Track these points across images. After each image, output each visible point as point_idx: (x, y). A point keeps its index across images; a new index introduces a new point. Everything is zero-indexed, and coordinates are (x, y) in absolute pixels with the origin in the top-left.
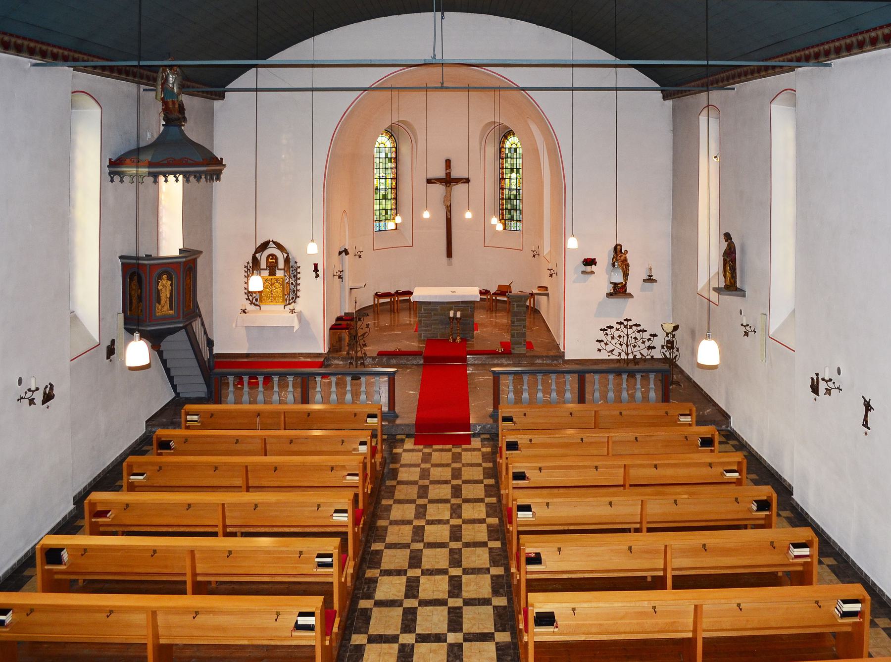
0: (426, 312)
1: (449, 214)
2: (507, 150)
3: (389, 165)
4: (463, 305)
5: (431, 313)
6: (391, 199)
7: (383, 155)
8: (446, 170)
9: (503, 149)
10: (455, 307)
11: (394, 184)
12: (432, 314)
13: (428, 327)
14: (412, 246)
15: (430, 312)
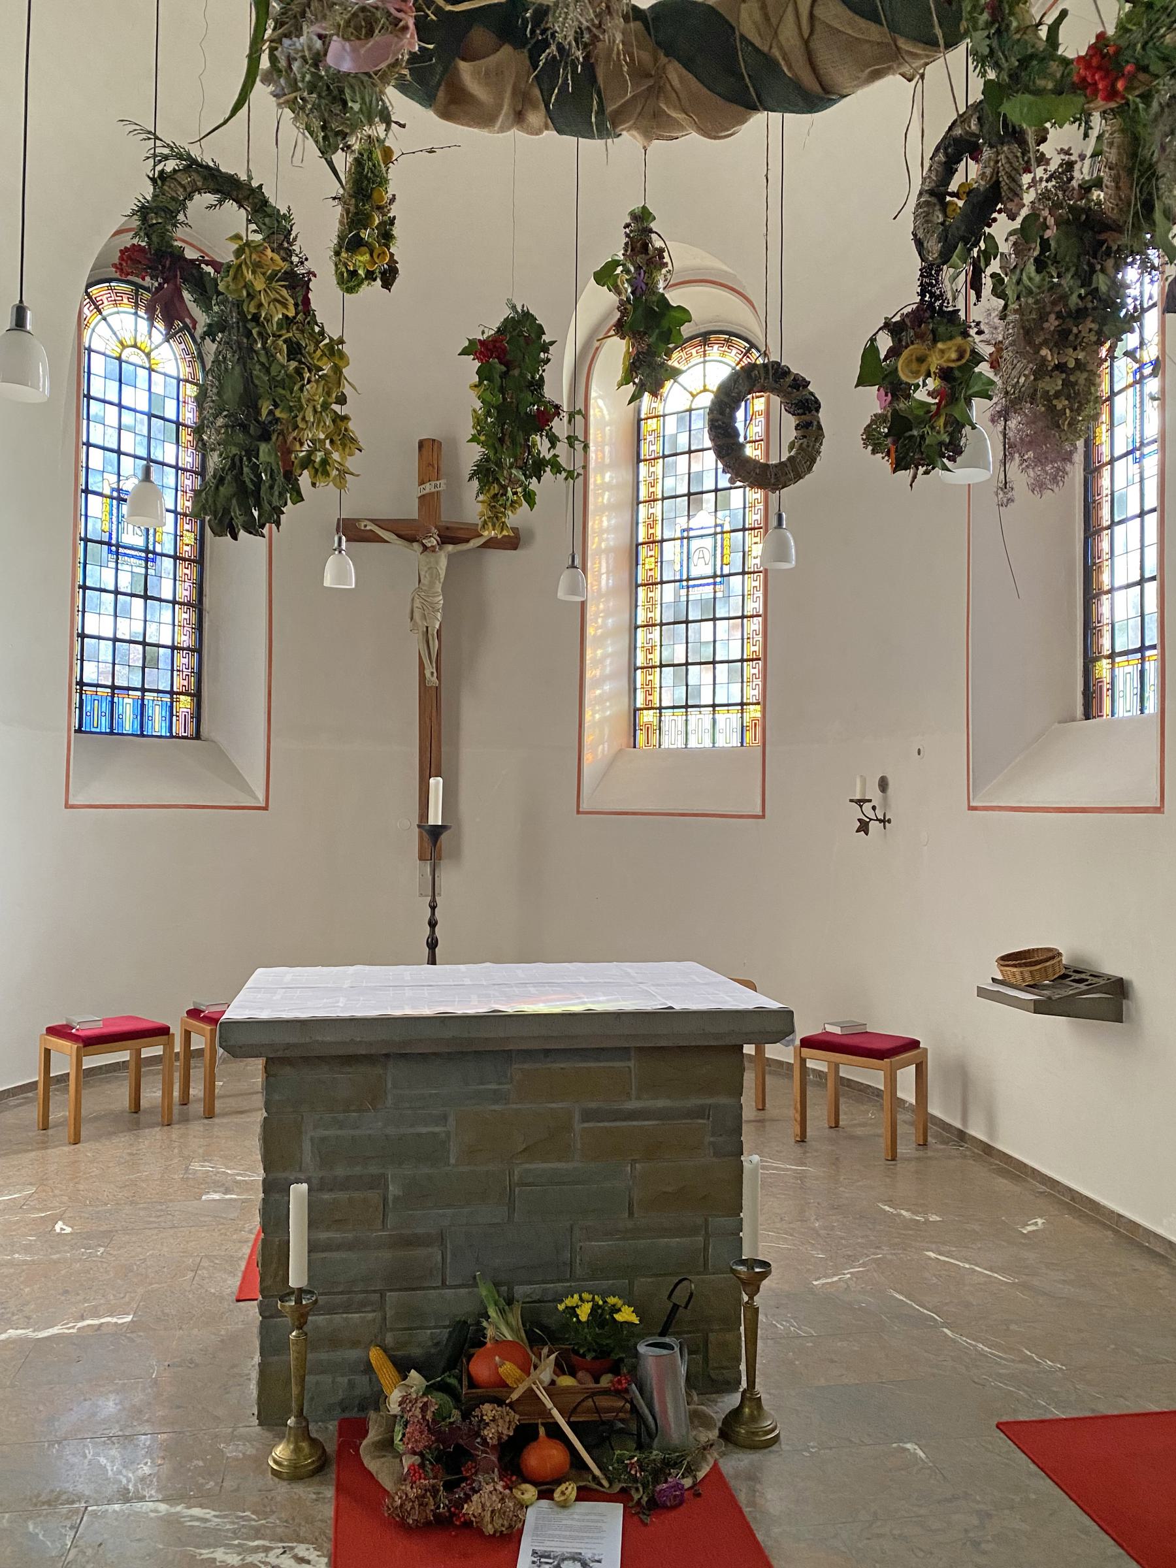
0: (340, 1171)
1: (429, 670)
2: (671, 423)
3: (167, 452)
4: (661, 1103)
5: (378, 1182)
6: (174, 602)
7: (136, 397)
8: (422, 483)
9: (652, 424)
10: (588, 1116)
11: (189, 538)
12: (393, 1190)
13: (347, 1308)
14: (266, 808)
15: (373, 1170)
